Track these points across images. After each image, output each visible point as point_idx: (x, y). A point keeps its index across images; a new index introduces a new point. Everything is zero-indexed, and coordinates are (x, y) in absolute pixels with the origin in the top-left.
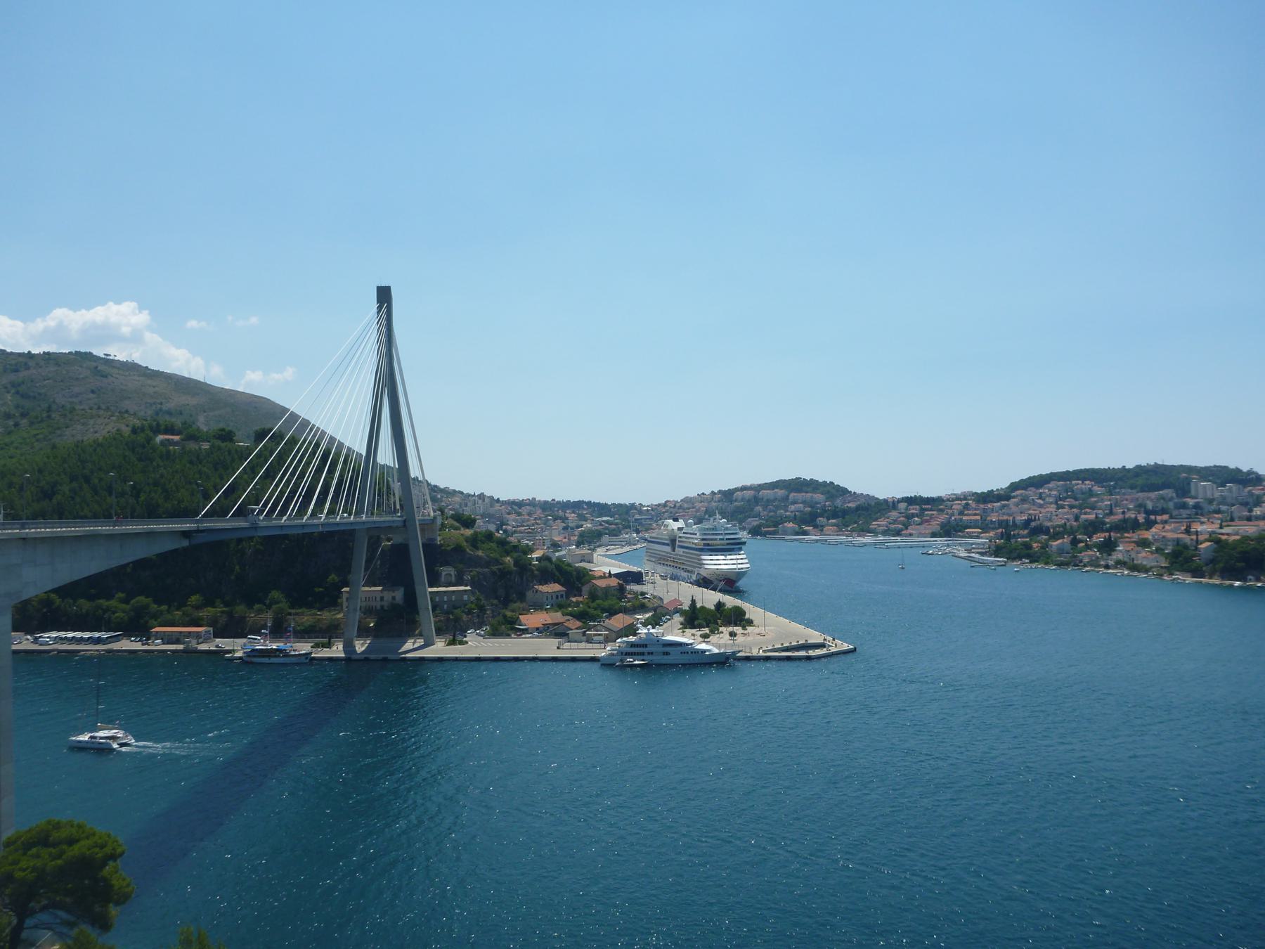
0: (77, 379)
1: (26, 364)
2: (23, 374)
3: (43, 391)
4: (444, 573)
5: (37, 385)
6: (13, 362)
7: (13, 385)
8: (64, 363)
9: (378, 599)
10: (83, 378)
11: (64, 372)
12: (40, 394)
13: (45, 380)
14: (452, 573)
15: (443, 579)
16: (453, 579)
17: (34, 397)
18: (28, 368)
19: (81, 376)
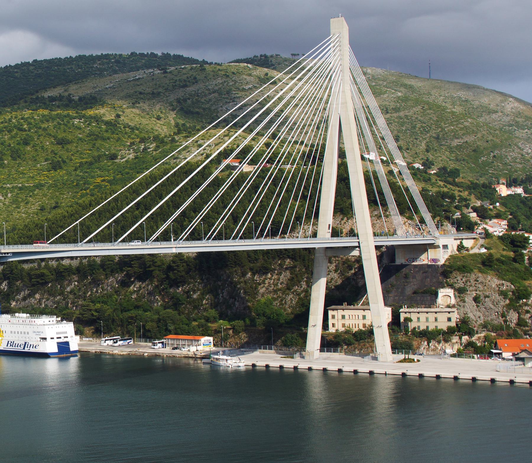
0: (244, 90)
1: (195, 78)
2: (191, 89)
3: (207, 106)
4: (440, 295)
5: (203, 100)
6: (184, 77)
7: (178, 101)
8: (233, 73)
9: (361, 317)
10: (250, 89)
11: (231, 84)
12: (204, 109)
13: (210, 94)
14: (452, 295)
15: (440, 300)
16: (453, 301)
17: (198, 113)
18: (195, 81)
19: (247, 87)
